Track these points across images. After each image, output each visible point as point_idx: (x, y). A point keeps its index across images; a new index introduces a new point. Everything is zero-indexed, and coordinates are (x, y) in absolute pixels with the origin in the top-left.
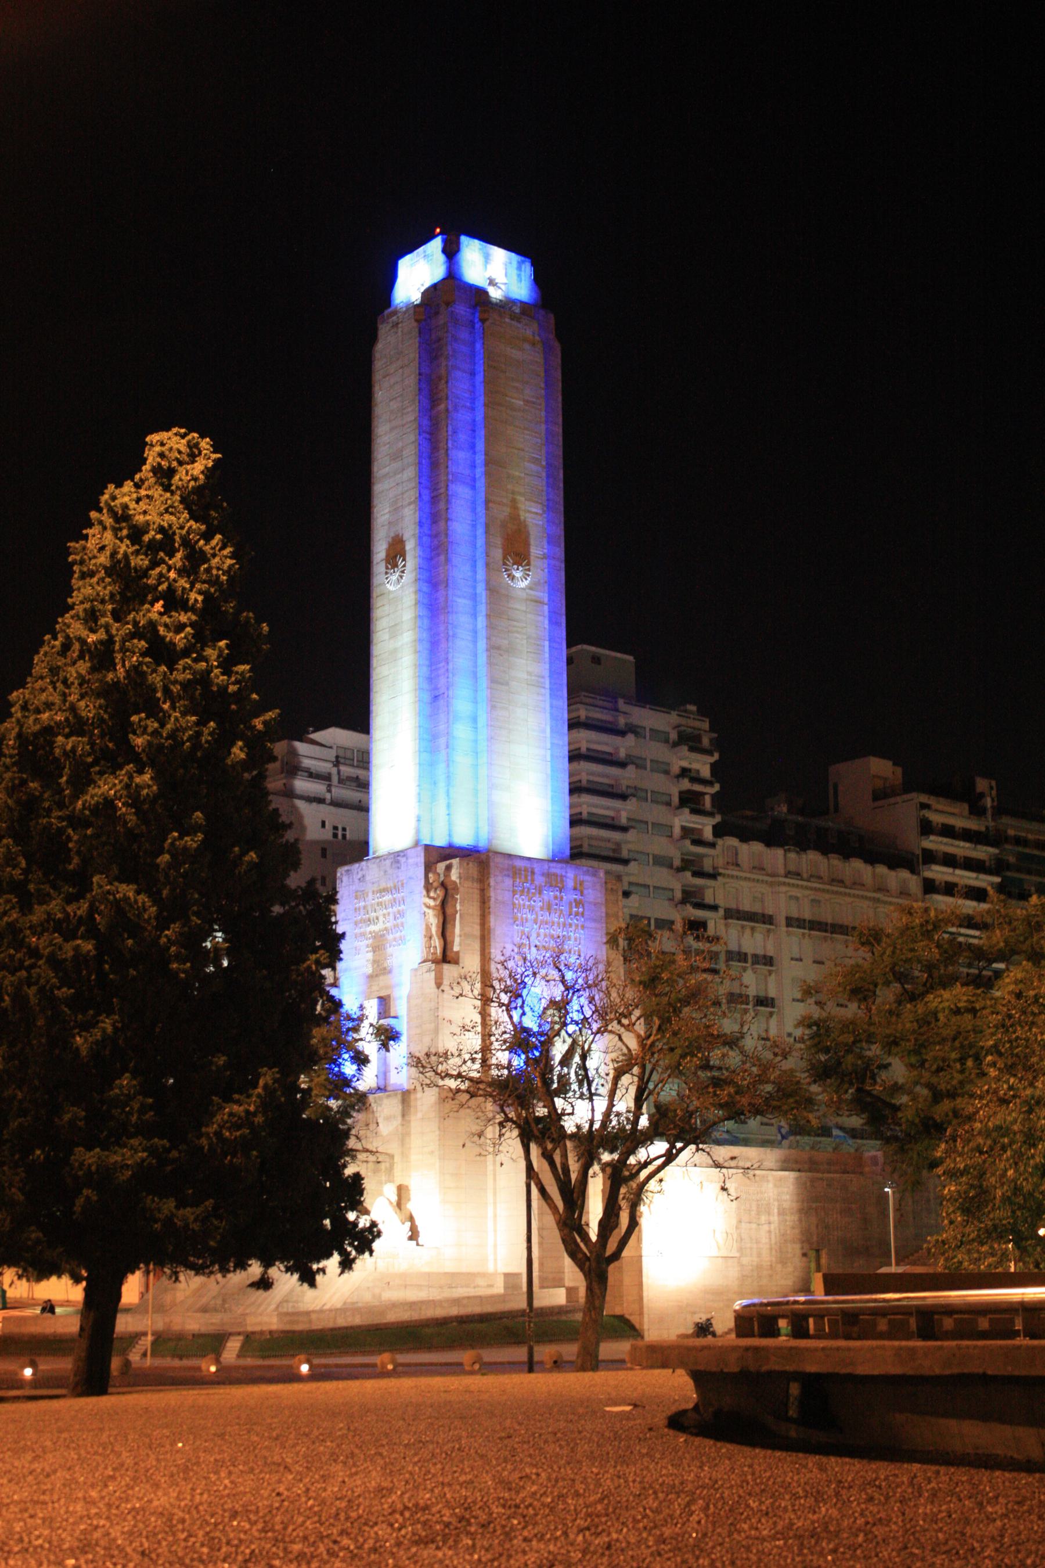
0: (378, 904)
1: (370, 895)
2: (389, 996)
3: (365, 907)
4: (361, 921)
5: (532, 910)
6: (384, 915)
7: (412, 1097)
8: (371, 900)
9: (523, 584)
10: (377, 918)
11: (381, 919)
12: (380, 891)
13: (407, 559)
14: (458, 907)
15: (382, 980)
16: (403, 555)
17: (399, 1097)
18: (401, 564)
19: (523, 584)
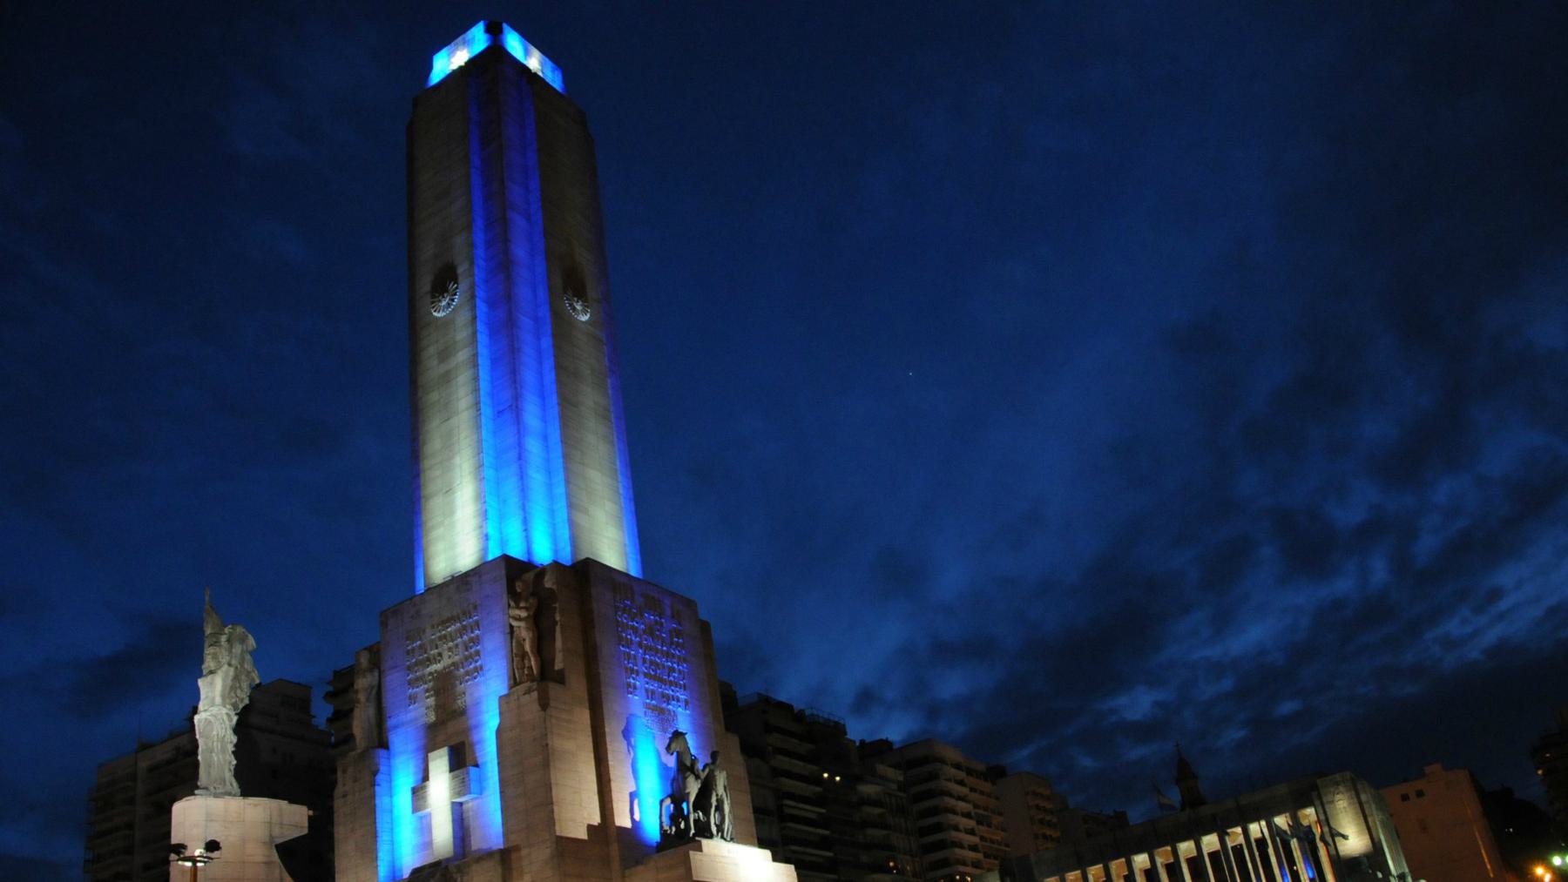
0: (440, 638)
1: (429, 631)
2: (463, 744)
3: (421, 647)
4: (416, 664)
5: (635, 631)
6: (450, 649)
7: (514, 856)
8: (430, 635)
9: (584, 318)
10: (440, 655)
11: (446, 654)
12: (443, 622)
13: (460, 279)
14: (558, 618)
15: (452, 727)
16: (455, 280)
17: (497, 857)
18: (452, 286)
19: (584, 318)
